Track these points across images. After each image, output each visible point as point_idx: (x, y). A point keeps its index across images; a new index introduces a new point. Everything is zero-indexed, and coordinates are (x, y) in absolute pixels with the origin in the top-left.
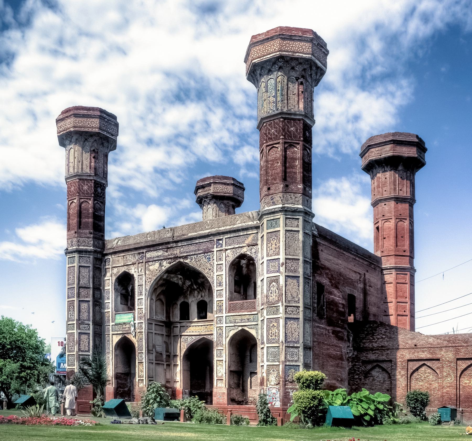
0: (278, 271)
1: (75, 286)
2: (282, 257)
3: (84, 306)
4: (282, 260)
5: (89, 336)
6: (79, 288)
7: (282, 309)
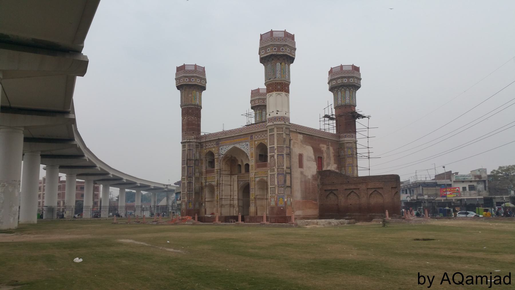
2: (275, 146)
4: (276, 147)
6: (187, 160)
7: (276, 170)
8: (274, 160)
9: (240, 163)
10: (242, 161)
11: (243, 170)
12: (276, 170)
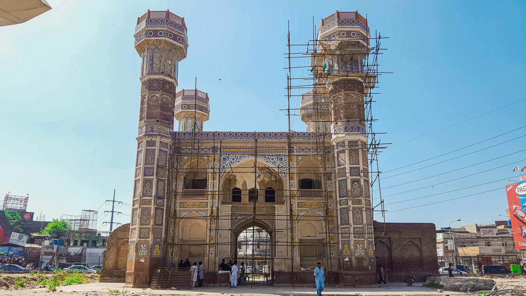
0: (359, 175)
1: (155, 166)
3: (161, 184)
5: (163, 211)
8: (360, 186)
9: (239, 185)
10: (245, 184)
11: (245, 198)
12: (363, 201)
